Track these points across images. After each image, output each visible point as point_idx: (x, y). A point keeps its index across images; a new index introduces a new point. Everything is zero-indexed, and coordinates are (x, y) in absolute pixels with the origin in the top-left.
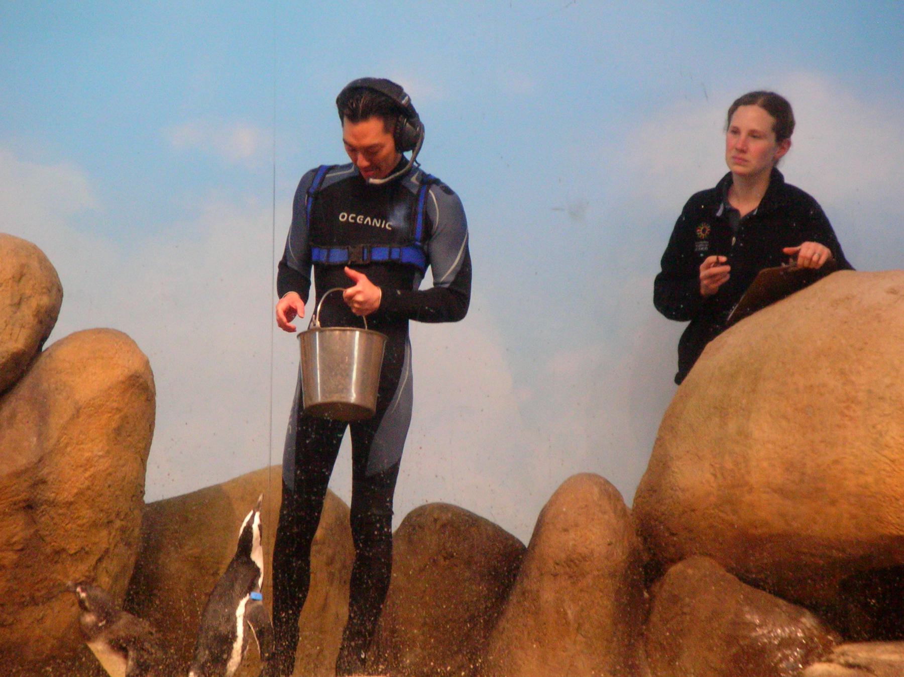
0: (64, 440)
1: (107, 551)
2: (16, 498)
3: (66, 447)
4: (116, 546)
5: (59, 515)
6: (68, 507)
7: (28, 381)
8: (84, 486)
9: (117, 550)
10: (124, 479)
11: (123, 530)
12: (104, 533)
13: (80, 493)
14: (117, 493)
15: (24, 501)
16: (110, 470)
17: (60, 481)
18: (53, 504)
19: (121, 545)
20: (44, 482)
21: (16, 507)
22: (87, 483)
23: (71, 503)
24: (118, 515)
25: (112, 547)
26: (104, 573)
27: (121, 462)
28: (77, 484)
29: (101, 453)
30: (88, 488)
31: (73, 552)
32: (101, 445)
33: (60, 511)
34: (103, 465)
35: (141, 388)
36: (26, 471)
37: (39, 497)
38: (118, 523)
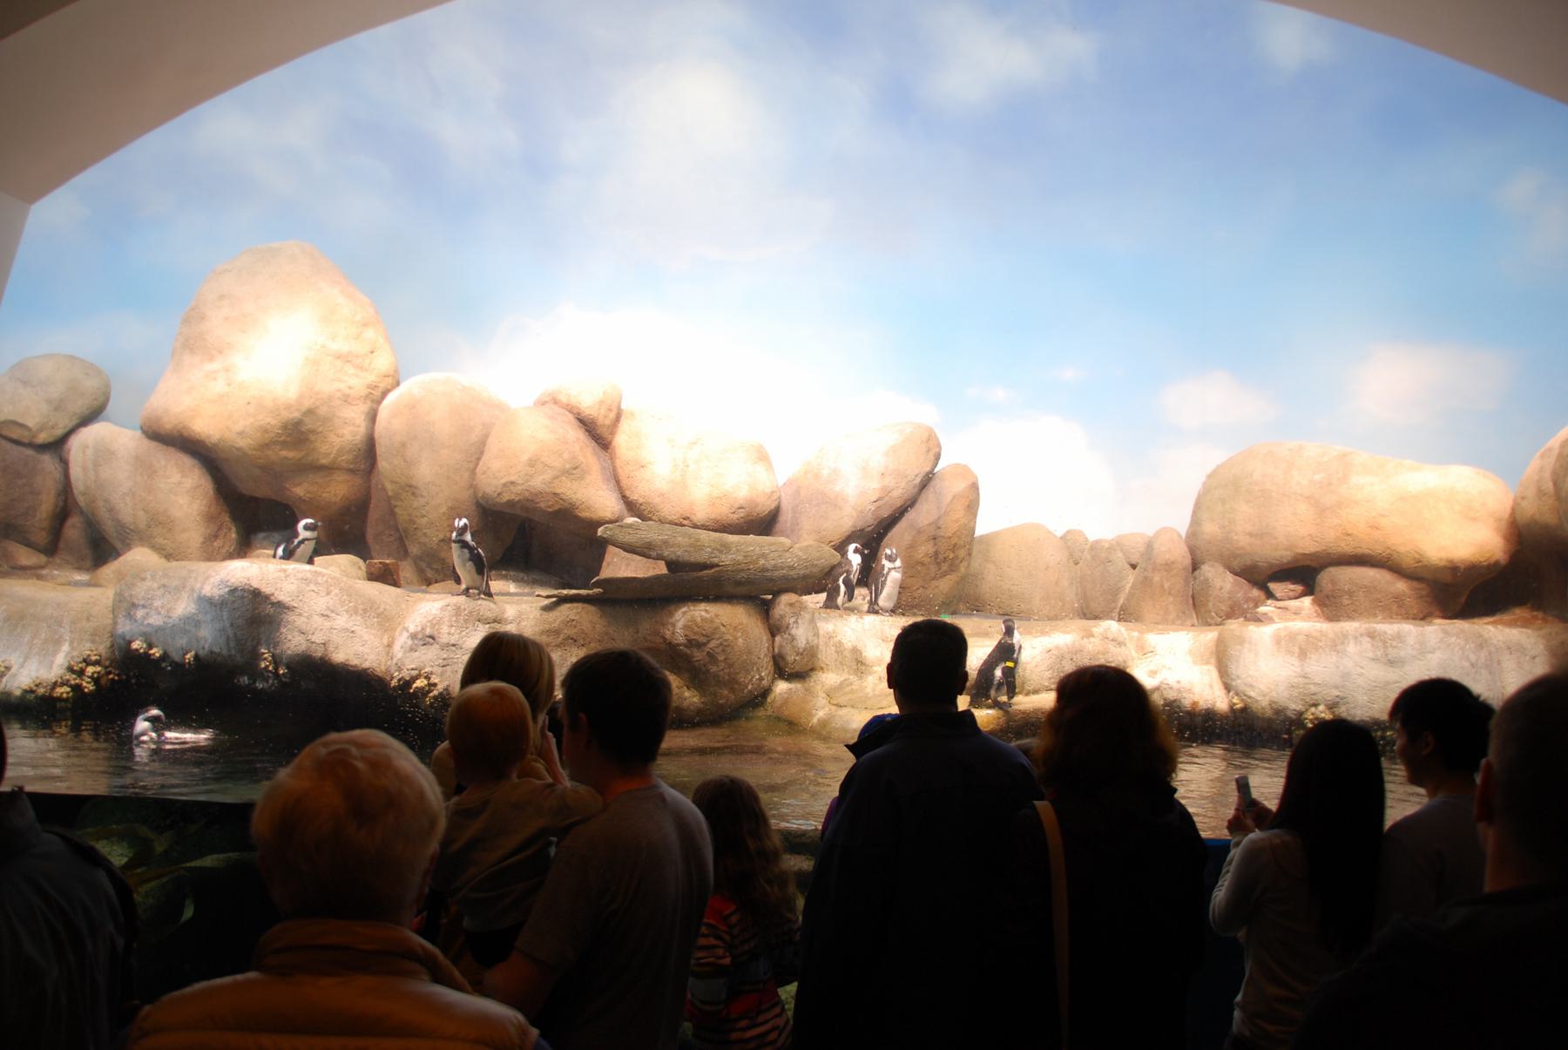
7: (933, 483)
34: (963, 521)
35: (974, 487)
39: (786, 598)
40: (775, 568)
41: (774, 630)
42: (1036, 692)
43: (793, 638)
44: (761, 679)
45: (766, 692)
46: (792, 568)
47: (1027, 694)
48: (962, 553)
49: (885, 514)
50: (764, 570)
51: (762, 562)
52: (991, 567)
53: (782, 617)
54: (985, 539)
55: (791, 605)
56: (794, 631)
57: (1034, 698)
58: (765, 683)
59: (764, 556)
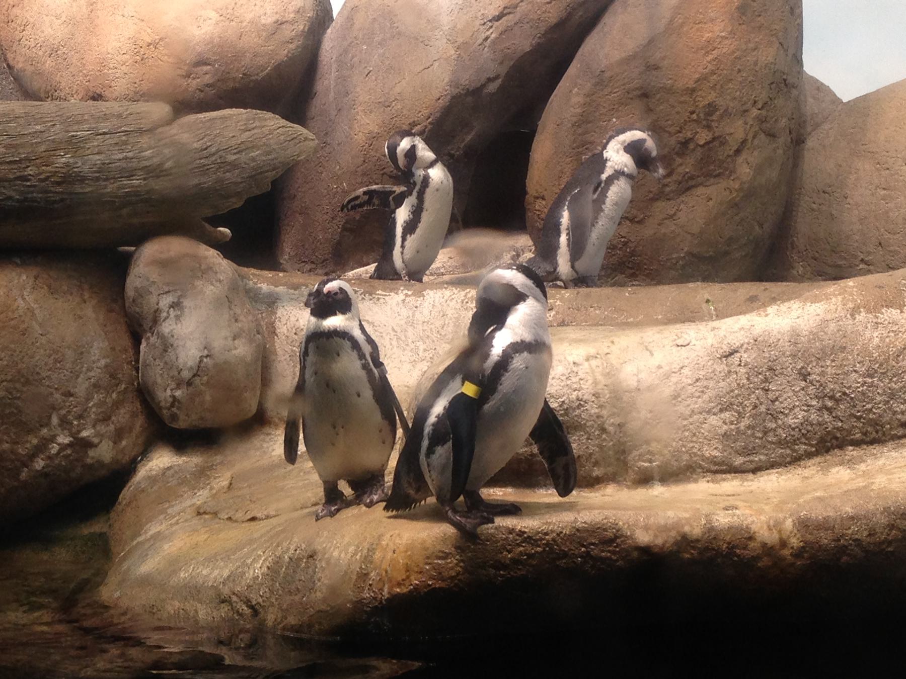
0: (679, 20)
1: (744, 142)
2: (627, 86)
3: (682, 25)
4: (754, 137)
5: (681, 102)
6: (691, 94)
8: (707, 71)
9: (756, 142)
10: (756, 64)
11: (762, 120)
12: (740, 122)
13: (704, 78)
14: (750, 78)
15: (637, 89)
16: (737, 54)
17: (677, 66)
18: (670, 91)
19: (763, 136)
20: (657, 68)
21: (630, 96)
22: (710, 67)
23: (694, 90)
24: (755, 102)
25: (750, 137)
26: (745, 165)
27: (751, 45)
28: (700, 69)
29: (723, 34)
30: (713, 73)
31: (702, 142)
32: (722, 24)
33: (682, 99)
34: (727, 47)
36: (634, 57)
37: (652, 84)
38: (755, 112)
39: (151, 250)
40: (103, 173)
41: (136, 327)
42: (673, 474)
43: (166, 346)
44: (86, 444)
45: (123, 473)
46: (155, 172)
47: (645, 480)
48: (736, 130)
49: (524, 43)
50: (69, 178)
51: (63, 160)
52: (865, 167)
53: (141, 293)
54: (864, 107)
55: (164, 264)
56: (166, 328)
57: (658, 491)
58: (105, 452)
59: (74, 144)
